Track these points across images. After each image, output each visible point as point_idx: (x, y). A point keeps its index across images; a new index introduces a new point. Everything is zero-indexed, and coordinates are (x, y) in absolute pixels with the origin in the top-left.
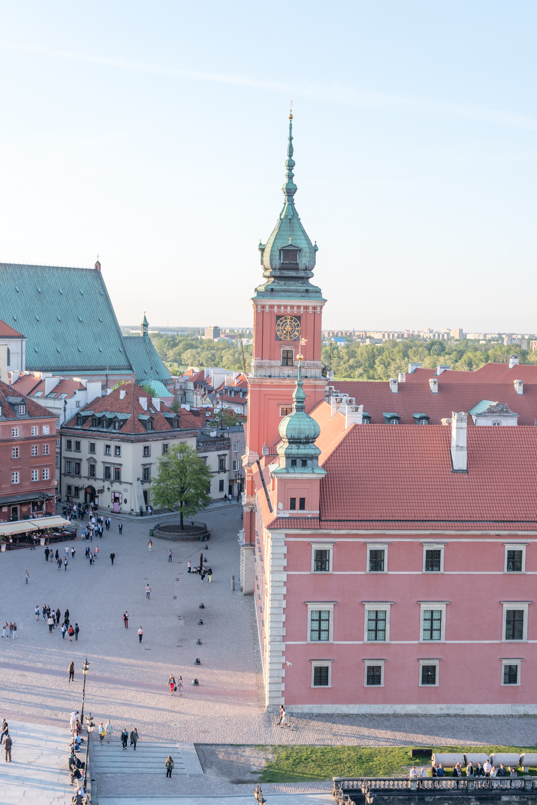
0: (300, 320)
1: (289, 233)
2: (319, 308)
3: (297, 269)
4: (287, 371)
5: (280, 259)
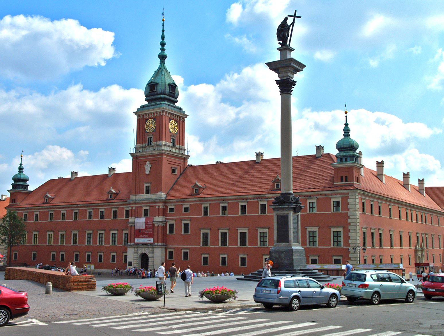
3: (173, 97)
4: (173, 150)
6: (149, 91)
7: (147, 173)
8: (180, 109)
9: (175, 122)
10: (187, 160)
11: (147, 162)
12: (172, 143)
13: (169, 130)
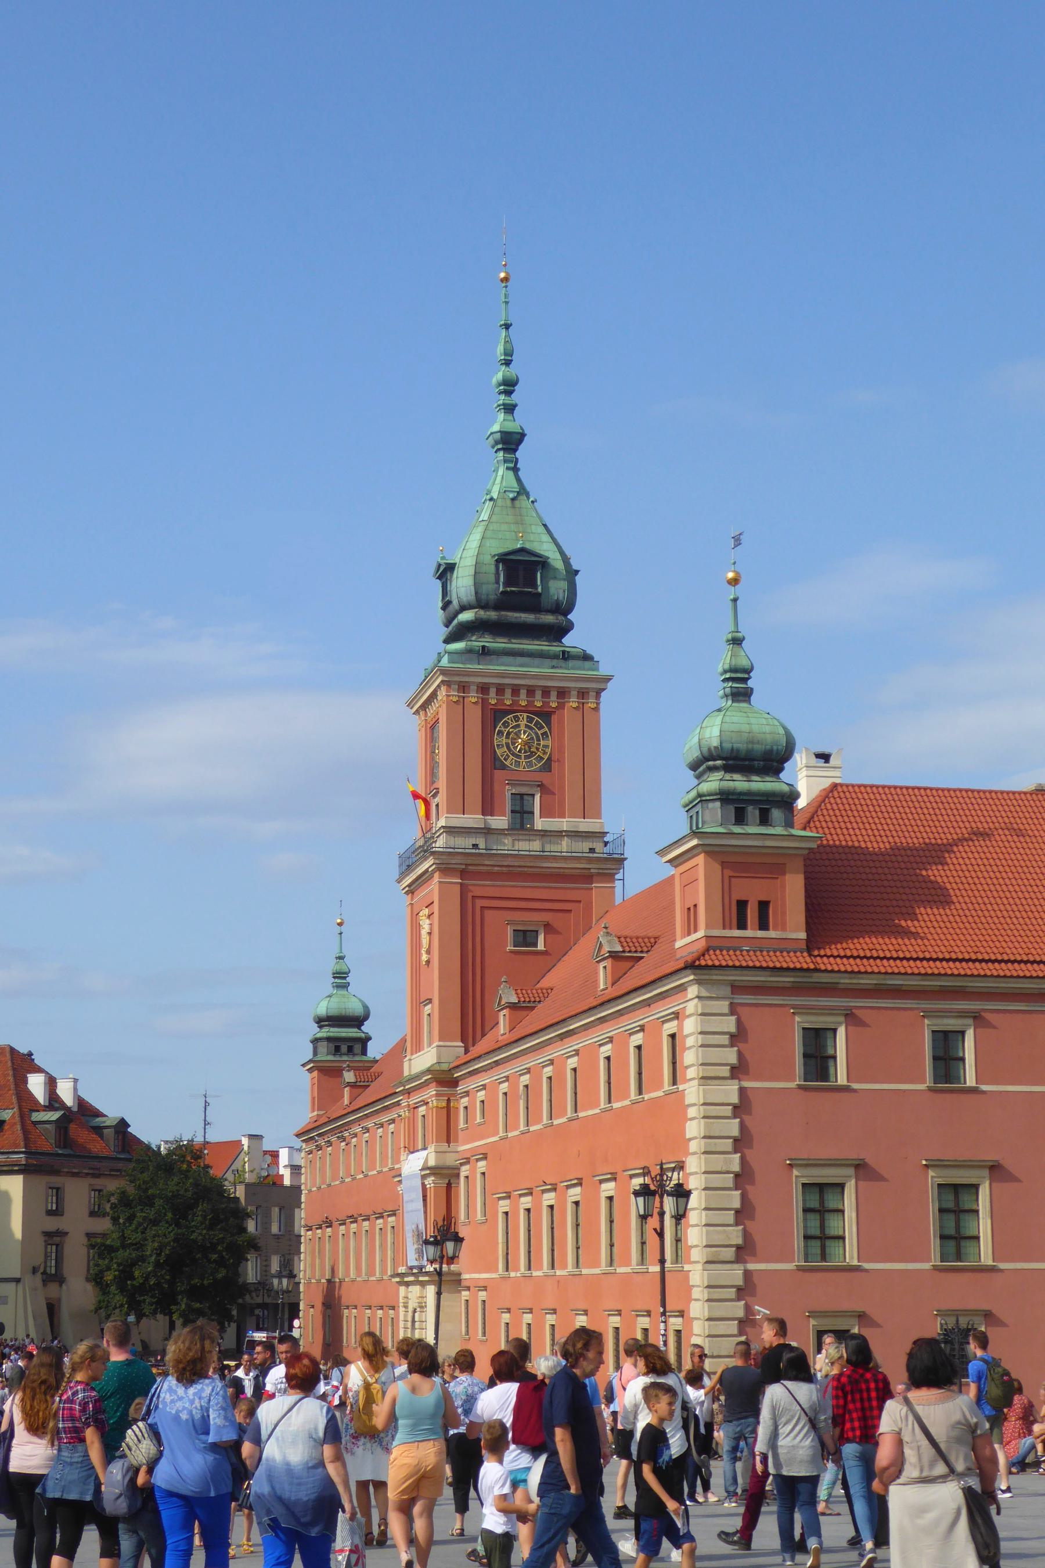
0: (549, 724)
1: (513, 527)
5: (497, 582)
7: (425, 957)
8: (566, 656)
10: (610, 877)
11: (421, 914)
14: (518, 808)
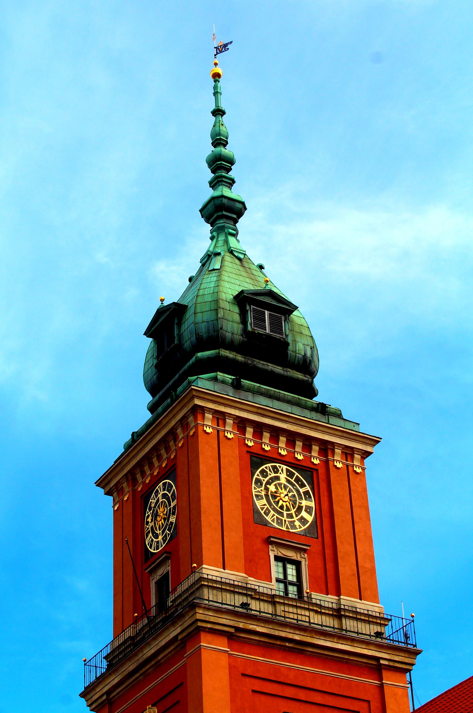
1: (248, 280)
2: (357, 457)
5: (244, 321)
6: (155, 362)
9: (297, 474)
12: (284, 581)
13: (255, 511)
14: (281, 577)
